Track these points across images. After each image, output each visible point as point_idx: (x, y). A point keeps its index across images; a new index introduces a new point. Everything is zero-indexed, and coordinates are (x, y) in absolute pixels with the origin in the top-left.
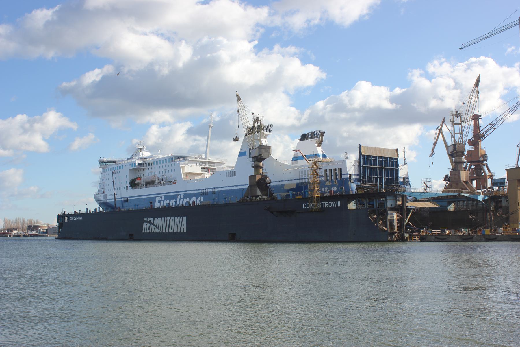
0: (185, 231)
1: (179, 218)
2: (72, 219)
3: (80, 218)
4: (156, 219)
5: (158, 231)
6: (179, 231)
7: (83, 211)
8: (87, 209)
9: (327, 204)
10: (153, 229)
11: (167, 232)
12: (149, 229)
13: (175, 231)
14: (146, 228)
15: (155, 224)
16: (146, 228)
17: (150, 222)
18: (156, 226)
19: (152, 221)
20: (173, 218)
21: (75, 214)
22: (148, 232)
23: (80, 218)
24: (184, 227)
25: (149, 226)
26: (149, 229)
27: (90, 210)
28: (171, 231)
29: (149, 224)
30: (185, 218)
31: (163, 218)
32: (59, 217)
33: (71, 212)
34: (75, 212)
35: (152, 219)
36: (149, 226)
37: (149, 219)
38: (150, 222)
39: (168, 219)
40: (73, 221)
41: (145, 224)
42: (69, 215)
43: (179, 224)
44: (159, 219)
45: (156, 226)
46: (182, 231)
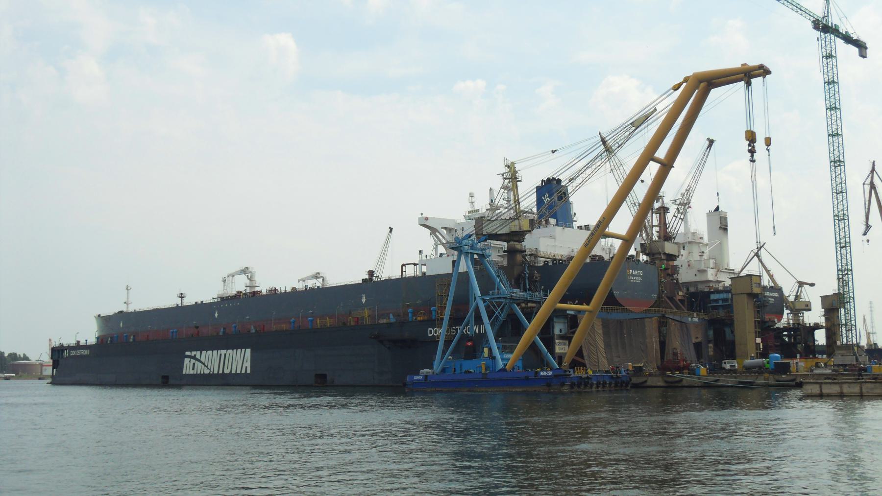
0: (249, 371)
1: (239, 350)
2: (73, 353)
4: (204, 352)
5: (207, 372)
6: (239, 372)
10: (200, 369)
11: (221, 372)
12: (193, 369)
13: (234, 372)
14: (188, 367)
15: (203, 360)
16: (188, 367)
17: (194, 357)
19: (198, 356)
20: (230, 351)
21: (78, 346)
22: (192, 372)
23: (86, 352)
24: (248, 364)
25: (194, 364)
26: (193, 369)
28: (227, 371)
29: (193, 361)
30: (248, 351)
31: (215, 352)
32: (54, 350)
33: (72, 342)
35: (199, 352)
36: (194, 364)
37: (193, 353)
38: (194, 357)
39: (223, 352)
40: (76, 357)
41: (187, 360)
42: (69, 348)
43: (239, 360)
44: (210, 352)
46: (243, 372)
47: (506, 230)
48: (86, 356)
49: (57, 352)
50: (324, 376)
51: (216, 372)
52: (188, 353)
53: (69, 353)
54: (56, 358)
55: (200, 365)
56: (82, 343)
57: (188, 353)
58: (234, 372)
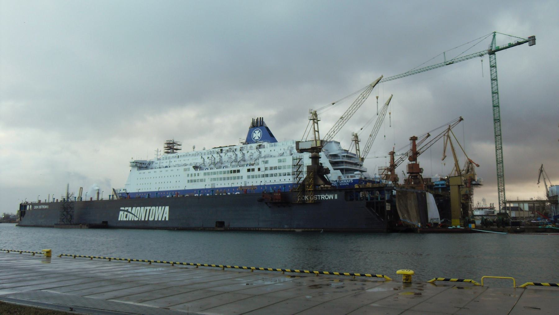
0: (167, 219)
1: (160, 207)
2: (36, 207)
3: (46, 207)
4: (134, 208)
5: (136, 219)
6: (160, 219)
9: (323, 197)
10: (131, 217)
11: (146, 219)
12: (126, 217)
13: (156, 219)
14: (122, 216)
15: (133, 212)
16: (122, 216)
17: (127, 211)
18: (134, 215)
20: (154, 208)
21: (39, 203)
22: (125, 219)
25: (127, 215)
26: (126, 217)
28: (151, 219)
29: (126, 213)
30: (167, 208)
31: (142, 208)
33: (36, 201)
34: (40, 201)
36: (127, 215)
37: (126, 208)
38: (127, 211)
39: (148, 208)
40: (38, 209)
41: (121, 213)
42: (33, 204)
43: (161, 213)
44: (139, 208)
45: (134, 215)
46: (163, 219)
47: (309, 147)
48: (46, 209)
51: (143, 219)
55: (131, 215)
56: (43, 201)
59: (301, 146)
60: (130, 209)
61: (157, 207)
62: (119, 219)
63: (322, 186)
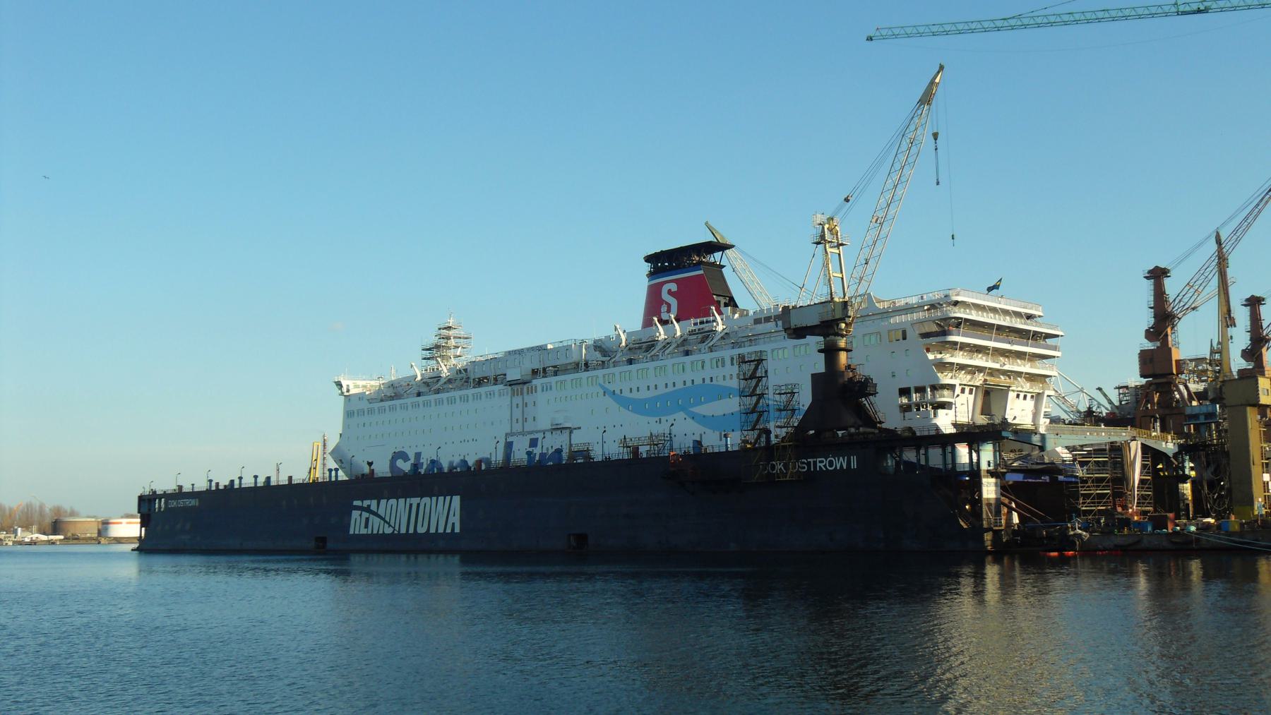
0: (457, 530)
2: (173, 504)
4: (383, 502)
5: (388, 531)
6: (441, 530)
7: (202, 485)
8: (211, 481)
9: (822, 463)
10: (376, 526)
11: (411, 531)
12: (366, 527)
13: (432, 530)
14: (358, 524)
15: (381, 512)
16: (358, 524)
17: (368, 509)
19: (374, 507)
20: (426, 500)
21: (179, 494)
22: (364, 531)
23: (193, 502)
24: (456, 519)
25: (367, 519)
26: (366, 527)
27: (217, 484)
28: (421, 530)
29: (365, 515)
30: (457, 500)
31: (402, 501)
32: (142, 499)
34: (180, 487)
35: (374, 502)
36: (367, 519)
37: (366, 503)
38: (368, 509)
39: (415, 501)
41: (355, 514)
42: (165, 495)
43: (443, 514)
44: (393, 501)
46: (449, 530)
49: (147, 506)
50: (582, 538)
51: (403, 531)
52: (357, 503)
53: (166, 503)
54: (145, 510)
55: (377, 520)
57: (357, 503)
58: (432, 530)
59: (796, 322)
60: (373, 504)
61: (434, 499)
62: (351, 532)
63: (853, 430)
